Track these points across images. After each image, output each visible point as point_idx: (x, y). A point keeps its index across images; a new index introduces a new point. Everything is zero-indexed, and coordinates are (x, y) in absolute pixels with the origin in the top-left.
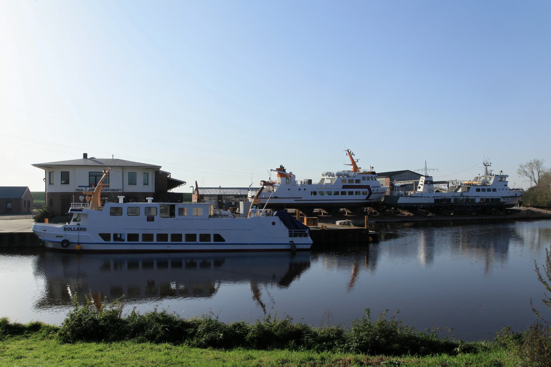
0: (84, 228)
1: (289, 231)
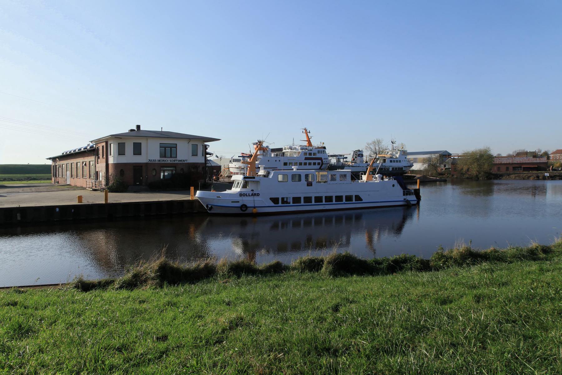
0: (257, 194)
1: (403, 191)
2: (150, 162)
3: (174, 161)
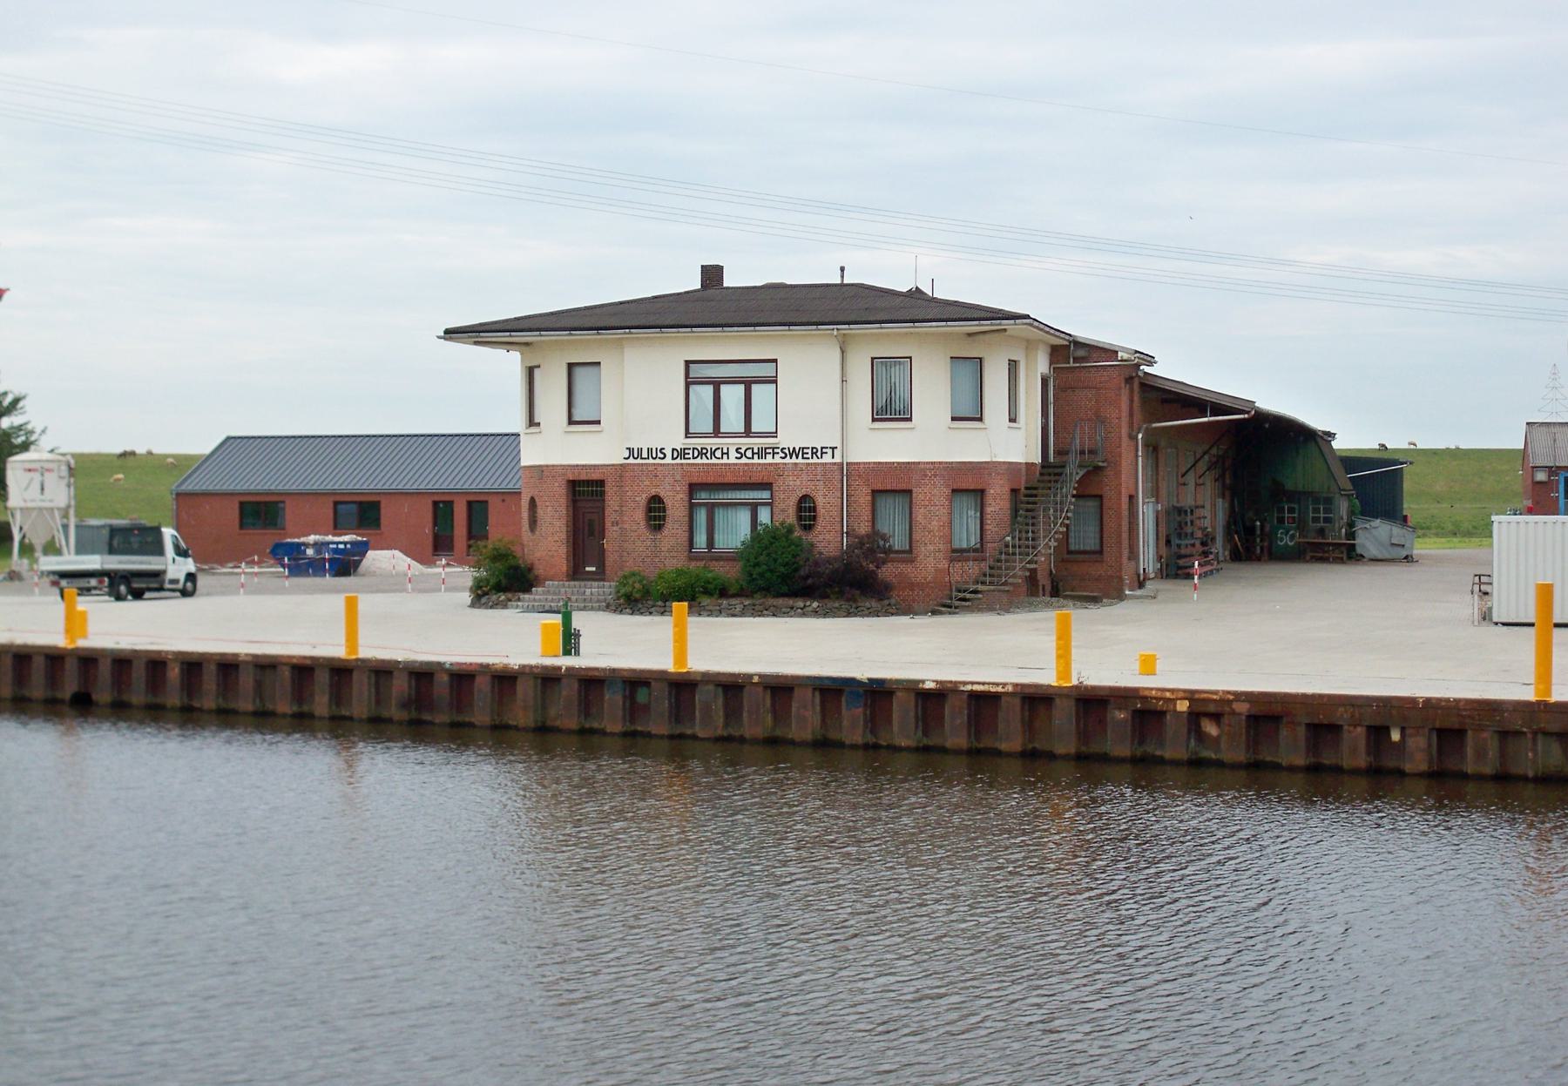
2: (631, 461)
3: (762, 452)
